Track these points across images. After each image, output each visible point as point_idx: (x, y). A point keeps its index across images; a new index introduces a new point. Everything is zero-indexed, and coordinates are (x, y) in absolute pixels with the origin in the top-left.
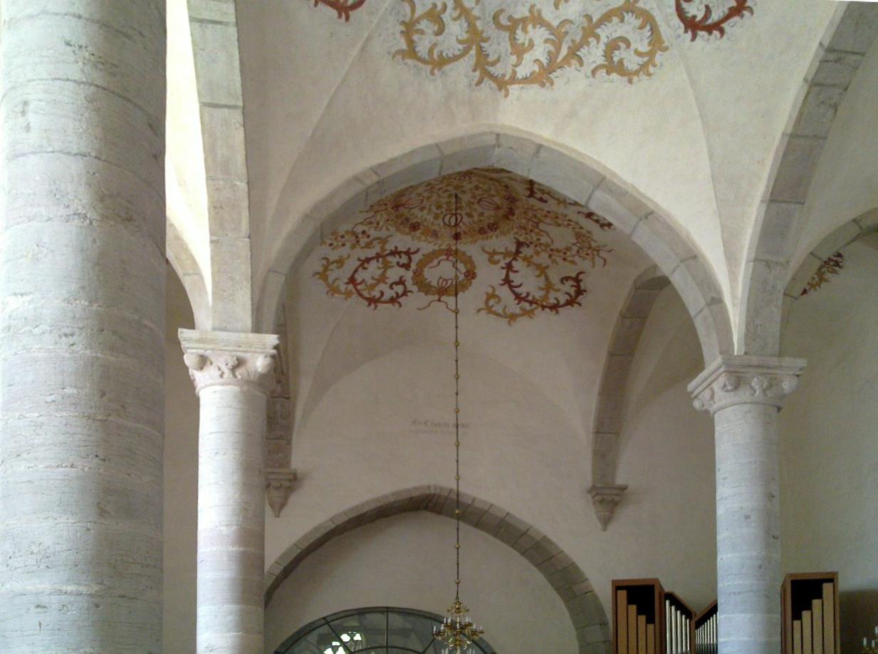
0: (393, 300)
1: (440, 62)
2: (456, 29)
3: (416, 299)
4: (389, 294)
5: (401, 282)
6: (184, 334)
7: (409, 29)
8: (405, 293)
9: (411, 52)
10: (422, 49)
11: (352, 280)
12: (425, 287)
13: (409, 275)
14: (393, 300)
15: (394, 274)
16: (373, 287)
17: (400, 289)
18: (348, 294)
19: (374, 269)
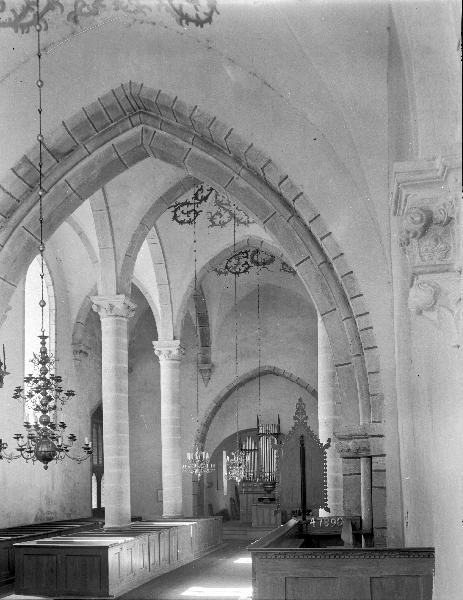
0: (245, 271)
1: (223, 224)
2: (226, 216)
3: (254, 269)
4: (243, 269)
5: (246, 263)
6: (154, 343)
7: (212, 219)
8: (249, 267)
9: (214, 224)
10: (217, 222)
11: (227, 267)
12: (257, 264)
13: (249, 260)
14: (245, 271)
15: (243, 261)
16: (235, 268)
17: (246, 266)
18: (226, 273)
19: (234, 261)
